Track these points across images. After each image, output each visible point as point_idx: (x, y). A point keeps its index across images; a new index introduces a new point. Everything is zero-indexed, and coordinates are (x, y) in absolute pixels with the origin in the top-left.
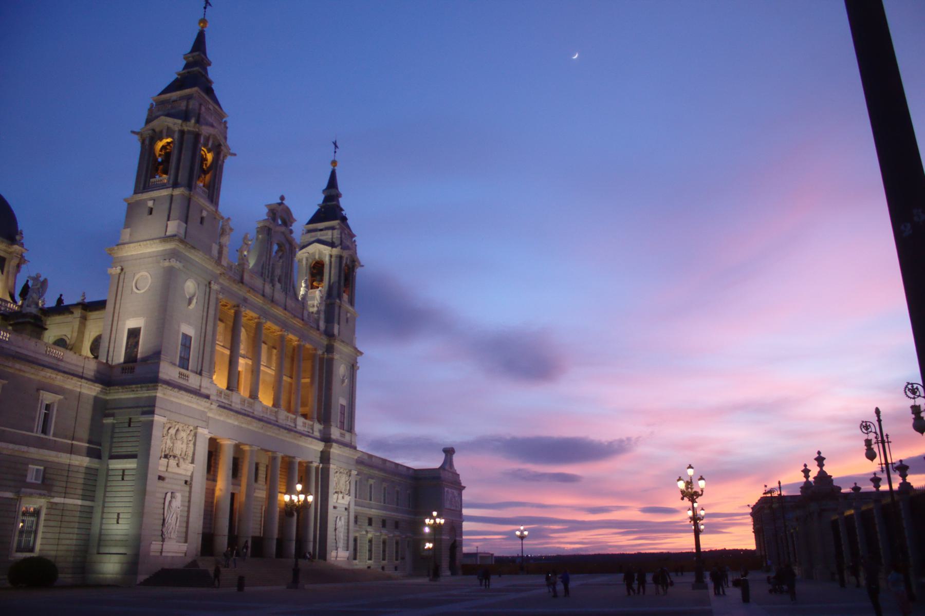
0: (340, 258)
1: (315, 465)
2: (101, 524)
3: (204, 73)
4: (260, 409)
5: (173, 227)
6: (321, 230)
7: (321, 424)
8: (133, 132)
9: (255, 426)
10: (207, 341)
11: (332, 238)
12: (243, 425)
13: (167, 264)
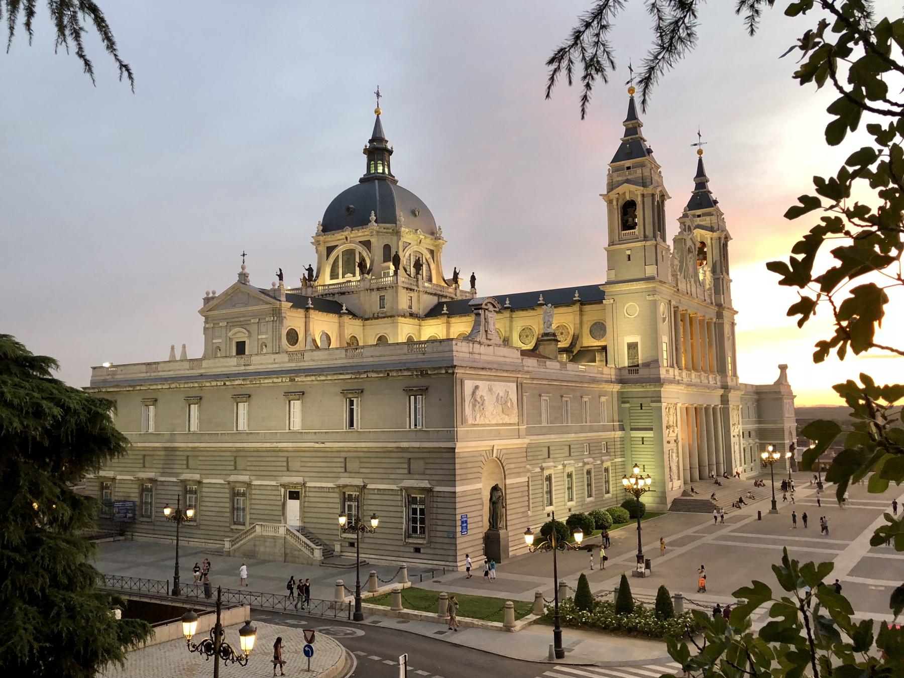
1: (720, 406)
6: (699, 216)
8: (601, 195)
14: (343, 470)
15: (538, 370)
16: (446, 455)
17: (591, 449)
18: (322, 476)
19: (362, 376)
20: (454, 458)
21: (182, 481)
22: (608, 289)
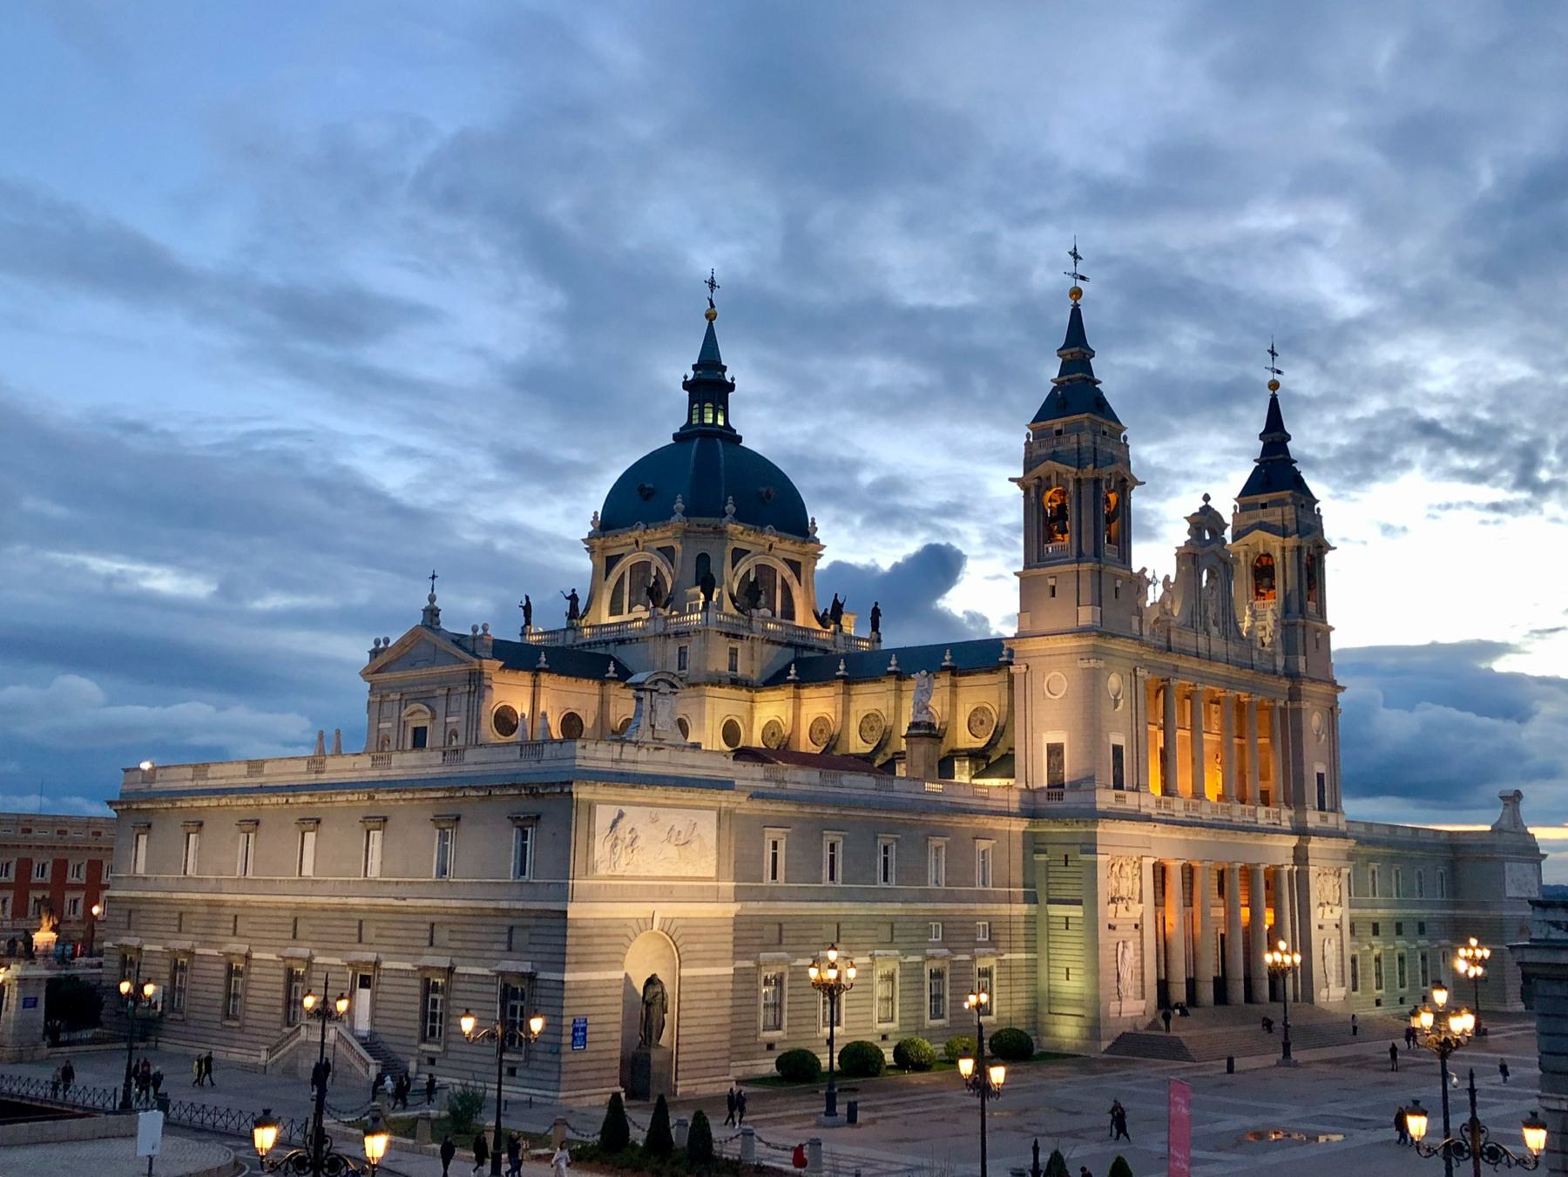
0: (1299, 548)
1: (1287, 868)
2: (1049, 979)
3: (1088, 377)
4: (1209, 811)
5: (1086, 616)
6: (1264, 506)
7: (1291, 809)
8: (1011, 480)
9: (1205, 836)
10: (1138, 743)
11: (1283, 520)
12: (1190, 838)
13: (1085, 664)
14: (427, 943)
15: (820, 789)
16: (555, 923)
17: (992, 931)
18: (401, 952)
19: (457, 794)
20: (566, 927)
21: (227, 955)
22: (1019, 647)
